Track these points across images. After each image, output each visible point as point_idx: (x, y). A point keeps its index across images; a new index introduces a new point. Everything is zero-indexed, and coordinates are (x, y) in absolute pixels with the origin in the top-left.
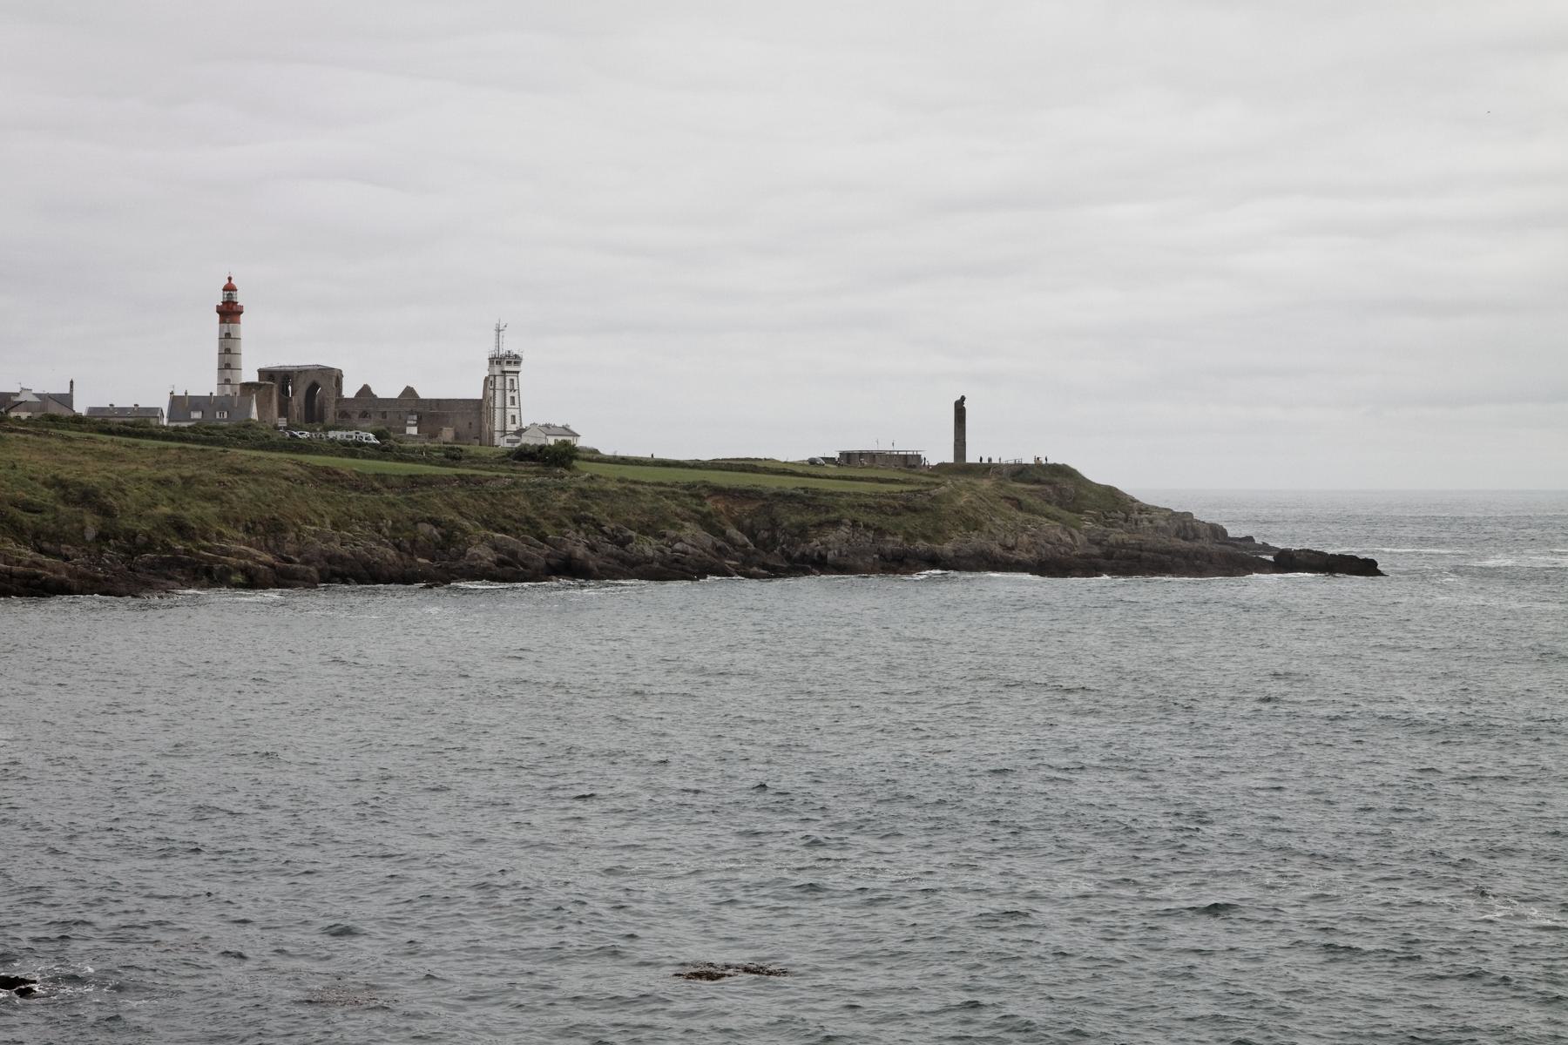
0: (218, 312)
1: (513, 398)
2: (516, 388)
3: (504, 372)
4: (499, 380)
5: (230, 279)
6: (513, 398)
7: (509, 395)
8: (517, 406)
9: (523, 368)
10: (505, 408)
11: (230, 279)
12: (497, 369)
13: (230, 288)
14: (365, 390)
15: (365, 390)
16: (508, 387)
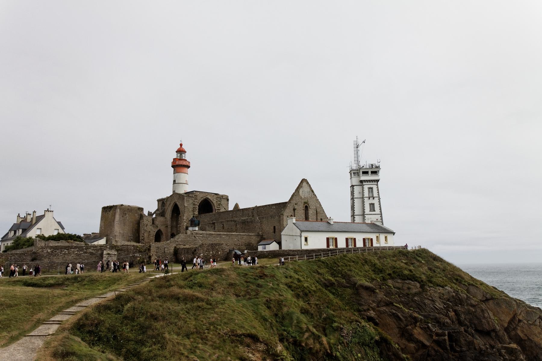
0: (172, 166)
1: (372, 206)
2: (375, 194)
3: (361, 182)
4: (357, 189)
5: (181, 145)
6: (372, 206)
7: (367, 203)
8: (377, 211)
9: (381, 176)
10: (363, 215)
11: (181, 145)
12: (355, 181)
13: (181, 151)
14: (237, 206)
15: (237, 206)
16: (366, 194)
